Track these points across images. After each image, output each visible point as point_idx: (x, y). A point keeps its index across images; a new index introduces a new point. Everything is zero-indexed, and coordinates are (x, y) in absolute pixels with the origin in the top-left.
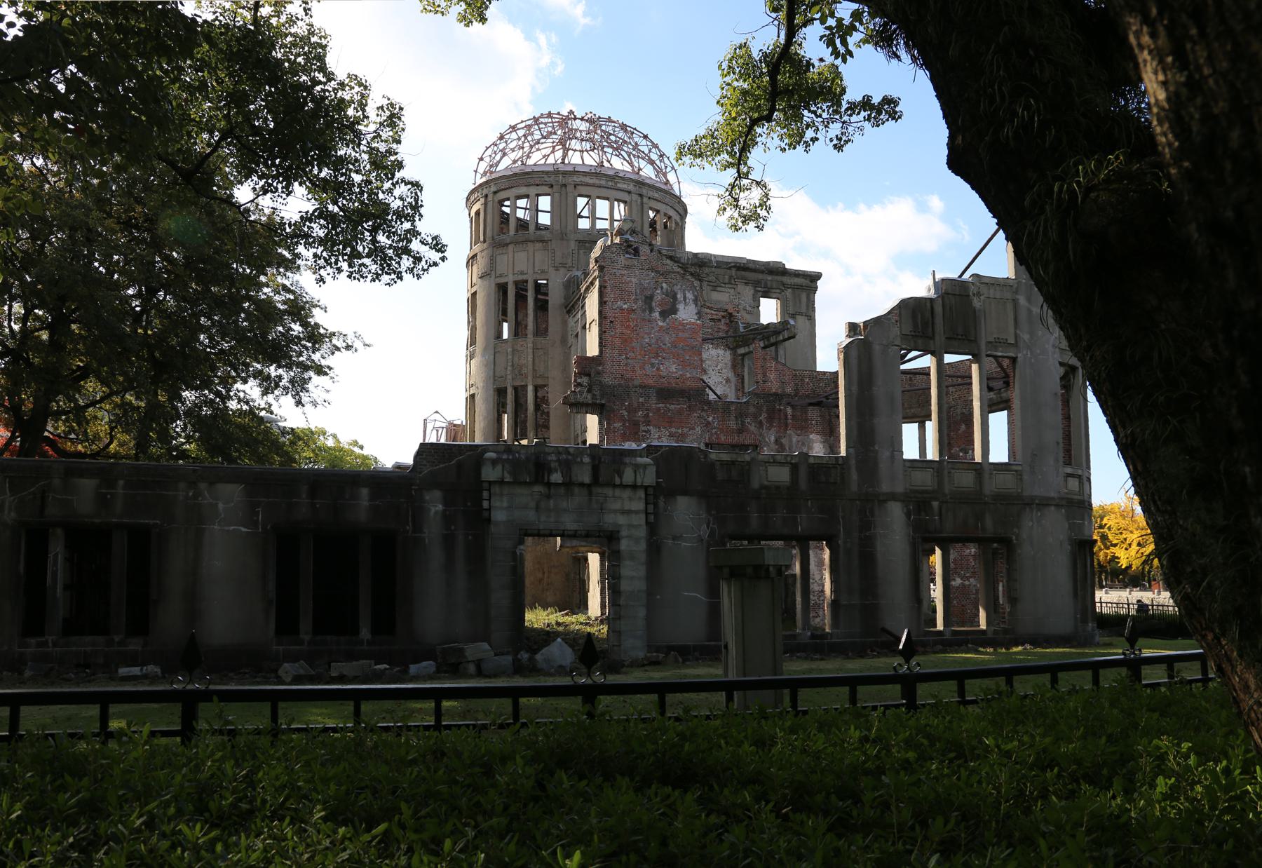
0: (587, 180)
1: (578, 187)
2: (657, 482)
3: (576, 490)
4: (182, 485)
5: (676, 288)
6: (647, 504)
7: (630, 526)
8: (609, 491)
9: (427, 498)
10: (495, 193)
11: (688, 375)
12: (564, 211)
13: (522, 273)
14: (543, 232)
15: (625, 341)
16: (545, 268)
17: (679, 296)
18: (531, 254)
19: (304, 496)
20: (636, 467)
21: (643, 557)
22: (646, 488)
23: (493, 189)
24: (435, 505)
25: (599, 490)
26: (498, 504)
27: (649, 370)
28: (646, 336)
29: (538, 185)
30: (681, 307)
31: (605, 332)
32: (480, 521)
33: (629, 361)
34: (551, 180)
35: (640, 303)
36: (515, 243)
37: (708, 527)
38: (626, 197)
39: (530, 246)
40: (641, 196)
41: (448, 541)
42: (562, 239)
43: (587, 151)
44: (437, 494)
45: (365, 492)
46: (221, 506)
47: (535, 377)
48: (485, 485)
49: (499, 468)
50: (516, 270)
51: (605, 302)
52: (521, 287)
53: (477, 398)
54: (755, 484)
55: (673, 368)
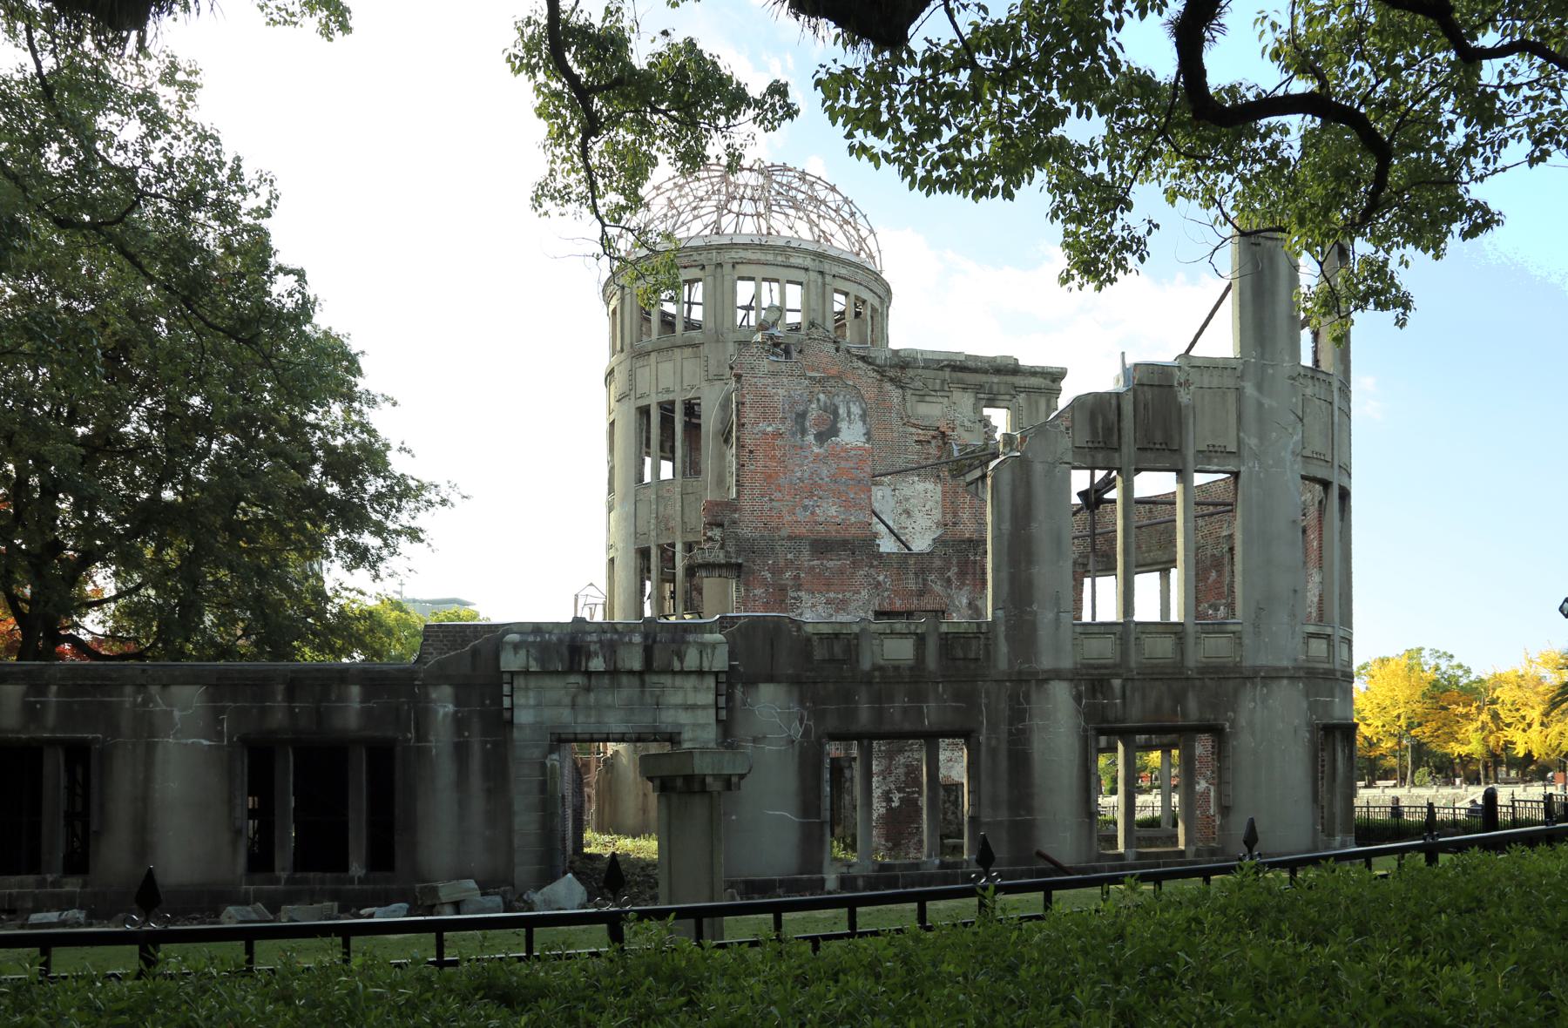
0: (749, 255)
1: (737, 266)
2: (730, 666)
3: (625, 680)
4: (129, 689)
5: (837, 400)
6: (717, 695)
7: (695, 725)
8: (667, 680)
9: (434, 696)
12: (721, 300)
14: (693, 333)
15: (769, 477)
17: (841, 411)
18: (679, 364)
19: (279, 698)
20: (702, 647)
22: (716, 674)
24: (443, 705)
25: (655, 679)
28: (797, 469)
30: (843, 425)
32: (500, 723)
33: (774, 503)
35: (789, 423)
37: (801, 724)
38: (801, 275)
40: (822, 273)
42: (717, 341)
44: (447, 691)
45: (355, 691)
46: (177, 714)
48: (506, 677)
49: (523, 653)
50: (661, 386)
52: (667, 409)
53: (616, 563)
54: (866, 665)
55: (833, 511)
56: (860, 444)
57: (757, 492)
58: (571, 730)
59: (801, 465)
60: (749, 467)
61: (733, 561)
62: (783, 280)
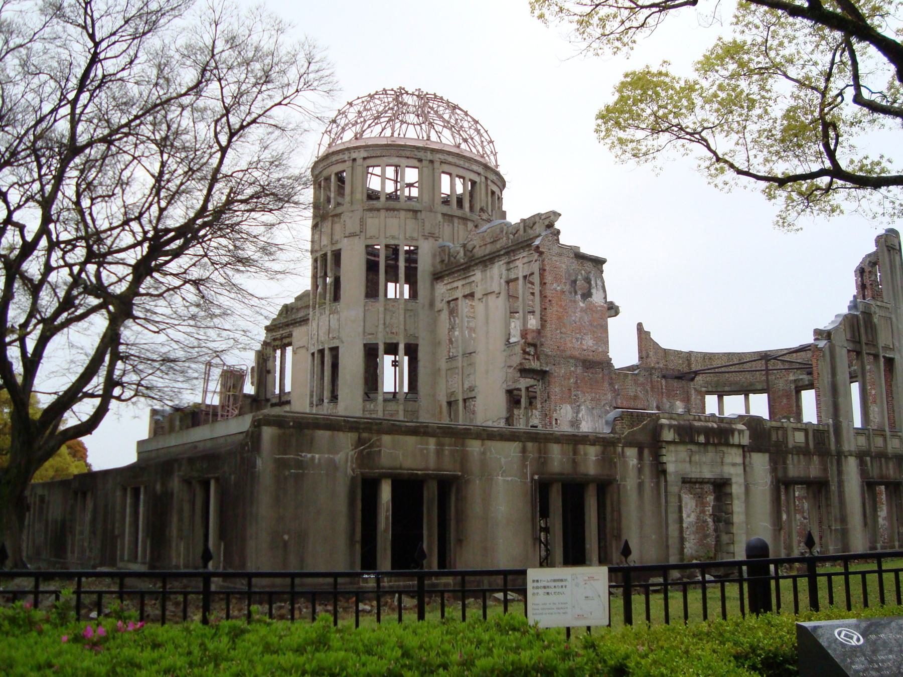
0: (450, 159)
7: (737, 475)
8: (725, 449)
10: (364, 159)
11: (600, 350)
13: (393, 238)
15: (559, 318)
16: (415, 235)
17: (593, 282)
20: (740, 432)
21: (743, 497)
22: (743, 447)
23: (363, 154)
27: (577, 345)
30: (594, 291)
32: (660, 471)
34: (421, 155)
36: (388, 209)
39: (403, 214)
41: (641, 485)
42: (431, 211)
46: (503, 460)
47: (406, 336)
49: (672, 430)
51: (545, 284)
57: (554, 326)
59: (575, 313)
60: (549, 311)
62: (467, 179)
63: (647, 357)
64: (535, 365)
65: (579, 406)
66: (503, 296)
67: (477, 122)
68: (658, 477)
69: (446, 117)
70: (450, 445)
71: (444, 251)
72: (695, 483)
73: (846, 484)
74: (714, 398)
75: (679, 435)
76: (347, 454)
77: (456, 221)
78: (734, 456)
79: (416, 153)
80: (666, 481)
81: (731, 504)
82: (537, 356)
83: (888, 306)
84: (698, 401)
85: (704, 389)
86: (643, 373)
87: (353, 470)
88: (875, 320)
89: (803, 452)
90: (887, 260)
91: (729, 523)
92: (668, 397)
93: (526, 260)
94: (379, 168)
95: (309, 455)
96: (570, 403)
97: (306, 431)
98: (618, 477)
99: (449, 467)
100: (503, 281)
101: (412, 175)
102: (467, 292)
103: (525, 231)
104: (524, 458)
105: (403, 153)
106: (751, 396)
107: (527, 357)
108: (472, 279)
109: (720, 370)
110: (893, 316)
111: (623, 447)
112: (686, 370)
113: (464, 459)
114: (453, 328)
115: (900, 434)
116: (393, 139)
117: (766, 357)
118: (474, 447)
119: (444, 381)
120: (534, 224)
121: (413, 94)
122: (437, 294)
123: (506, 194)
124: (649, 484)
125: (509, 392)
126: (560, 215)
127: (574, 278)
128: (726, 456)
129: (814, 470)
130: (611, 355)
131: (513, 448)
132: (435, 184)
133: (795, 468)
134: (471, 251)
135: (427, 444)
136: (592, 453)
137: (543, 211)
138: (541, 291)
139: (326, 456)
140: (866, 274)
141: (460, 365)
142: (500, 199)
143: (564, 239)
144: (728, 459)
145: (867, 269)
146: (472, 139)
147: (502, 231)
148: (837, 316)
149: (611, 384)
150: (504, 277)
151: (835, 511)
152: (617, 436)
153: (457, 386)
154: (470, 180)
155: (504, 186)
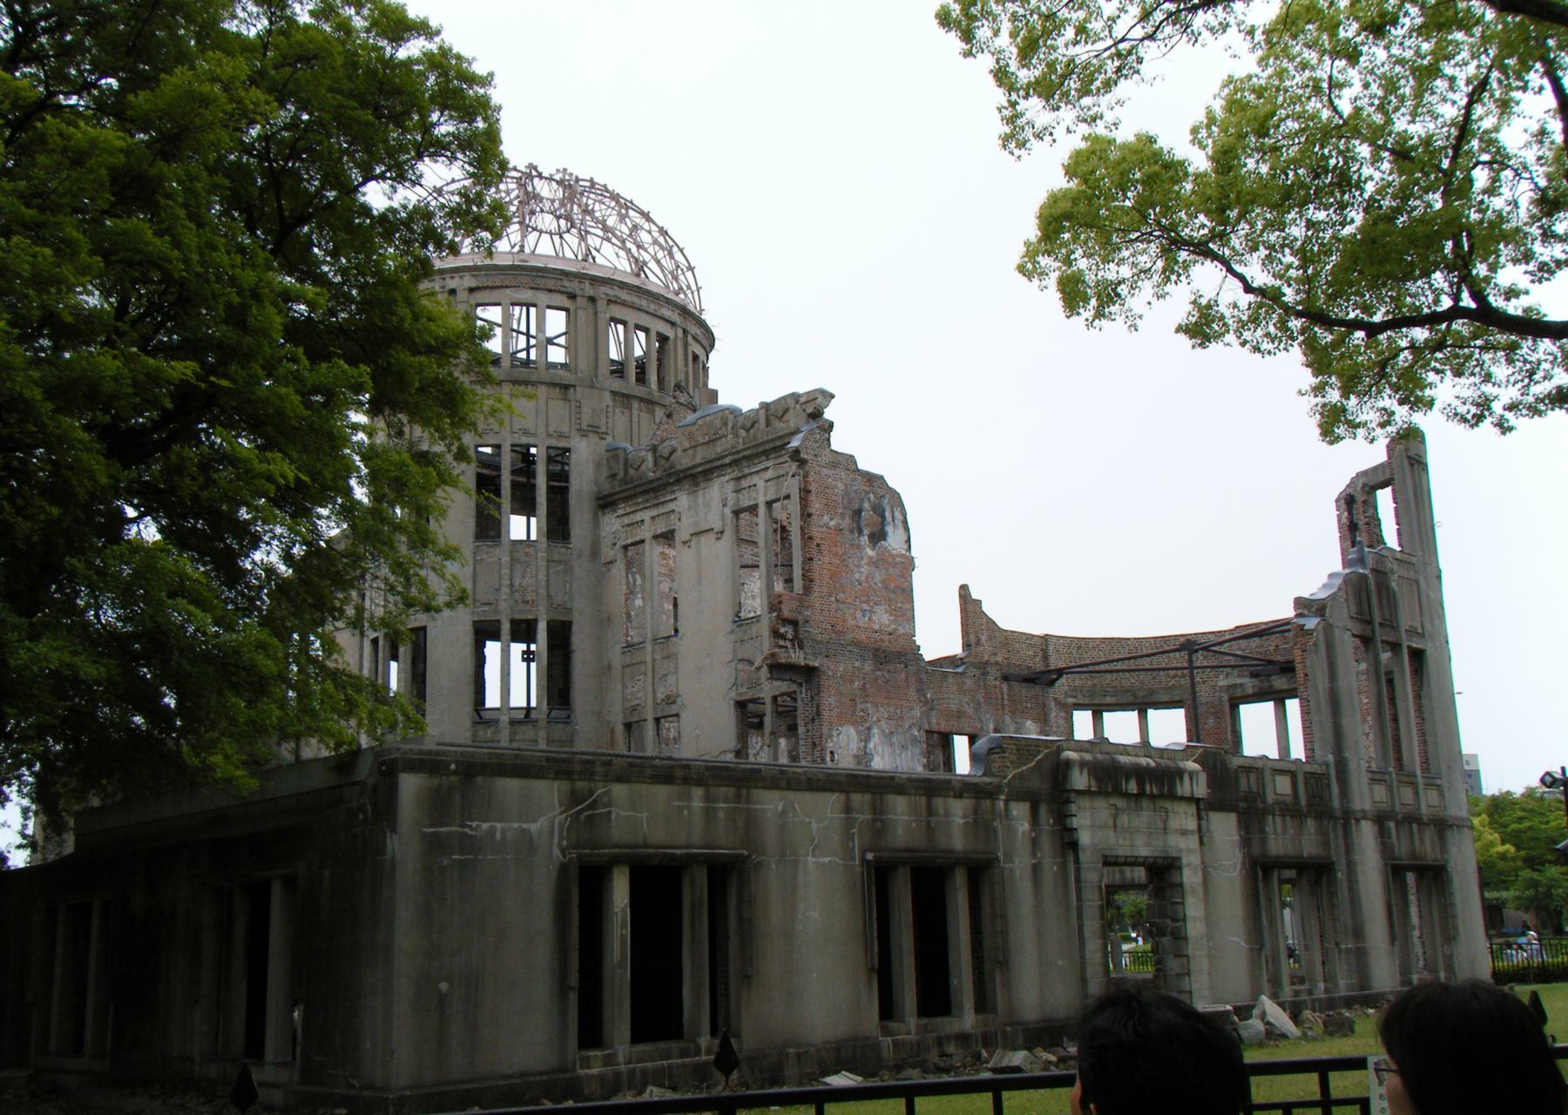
0: (624, 295)
1: (612, 306)
7: (1190, 851)
8: (1168, 805)
9: (1014, 813)
10: (471, 290)
11: (901, 631)
13: (526, 433)
16: (565, 429)
17: (887, 514)
20: (1191, 774)
21: (1200, 890)
22: (1197, 801)
23: (469, 282)
26: (1083, 822)
27: (863, 621)
29: (550, 291)
30: (889, 529)
31: (811, 559)
32: (1068, 844)
33: (841, 606)
35: (848, 520)
36: (516, 382)
39: (542, 391)
41: (1036, 869)
42: (592, 386)
43: (551, 234)
46: (814, 826)
51: (810, 515)
56: (903, 552)
58: (1115, 854)
59: (859, 566)
60: (816, 563)
61: (811, 663)
63: (978, 642)
64: (797, 657)
65: (869, 729)
66: (728, 536)
67: (663, 232)
68: (1063, 855)
69: (611, 222)
70: (726, 801)
71: (616, 457)
72: (1125, 864)
73: (1359, 869)
74: (1088, 714)
75: (1097, 778)
76: (553, 822)
77: (636, 405)
78: (1184, 817)
79: (566, 283)
80: (1077, 861)
81: (1182, 903)
82: (798, 642)
83: (1413, 560)
84: (1061, 722)
85: (1071, 700)
86: (973, 671)
87: (563, 852)
88: (1393, 584)
89: (1290, 810)
90: (1409, 481)
91: (1179, 937)
92: (1013, 712)
93: (769, 474)
94: (498, 309)
95: (485, 826)
96: (854, 724)
97: (479, 779)
98: (1000, 855)
99: (725, 843)
100: (728, 511)
101: (556, 322)
102: (661, 528)
103: (768, 424)
104: (849, 823)
105: (542, 283)
106: (1151, 712)
107: (781, 643)
108: (671, 506)
109: (1097, 668)
110: (1421, 579)
111: (1006, 802)
112: (1039, 667)
113: (751, 824)
114: (632, 593)
115: (1438, 782)
116: (522, 257)
117: (1189, 645)
118: (770, 803)
119: (619, 686)
120: (786, 411)
121: (550, 179)
122: (603, 534)
123: (715, 362)
124: (1050, 868)
125: (741, 705)
126: (832, 396)
127: (856, 506)
128: (1171, 816)
129: (1309, 846)
130: (919, 640)
131: (830, 803)
132: (599, 344)
133: (1280, 839)
134: (667, 459)
135: (690, 799)
136: (958, 810)
137: (802, 388)
138: (802, 529)
139: (516, 825)
140: (1358, 506)
141: (649, 659)
142: (706, 369)
143: (840, 442)
144: (1174, 824)
145: (1360, 498)
146: (658, 262)
147: (726, 424)
148: (1331, 576)
149: (921, 691)
150: (730, 504)
151: (1345, 915)
152: (995, 780)
153: (644, 694)
154: (659, 334)
155: (712, 346)
